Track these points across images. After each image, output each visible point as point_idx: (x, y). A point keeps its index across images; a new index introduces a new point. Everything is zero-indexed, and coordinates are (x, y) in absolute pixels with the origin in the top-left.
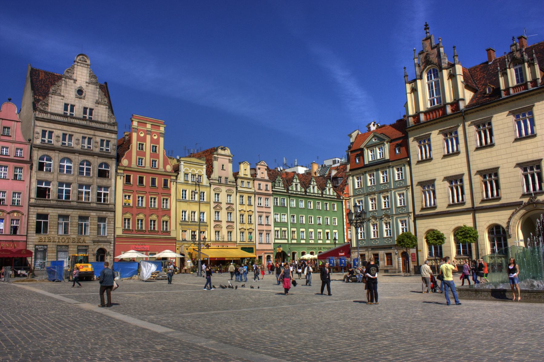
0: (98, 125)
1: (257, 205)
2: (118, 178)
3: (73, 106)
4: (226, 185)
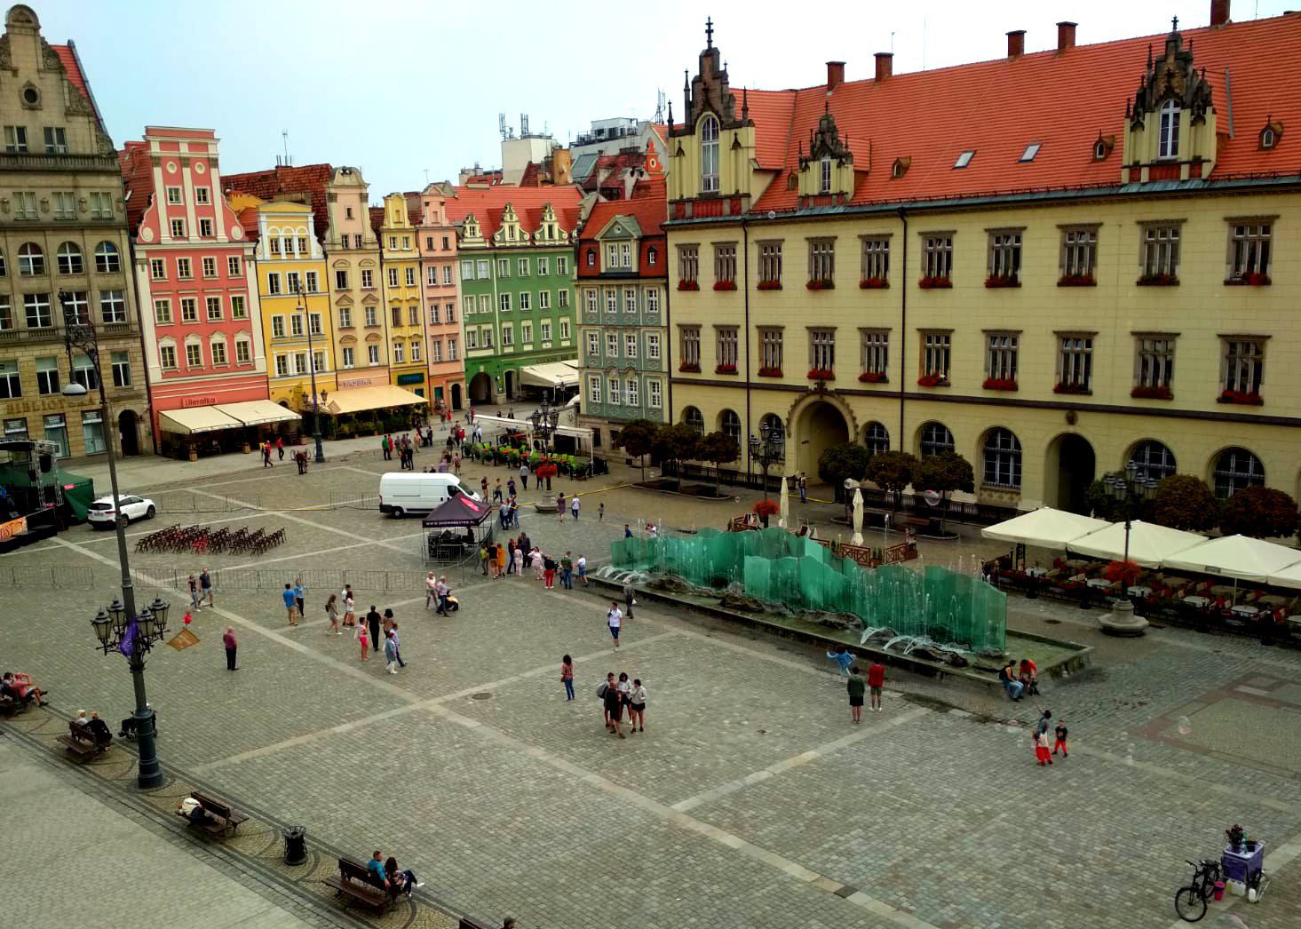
0: (78, 165)
1: (426, 283)
2: (139, 267)
3: (21, 131)
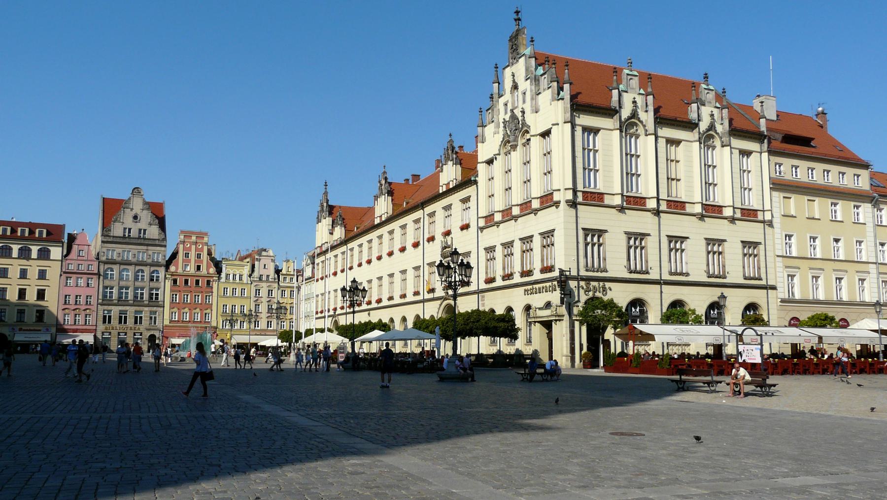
4: (267, 281)
